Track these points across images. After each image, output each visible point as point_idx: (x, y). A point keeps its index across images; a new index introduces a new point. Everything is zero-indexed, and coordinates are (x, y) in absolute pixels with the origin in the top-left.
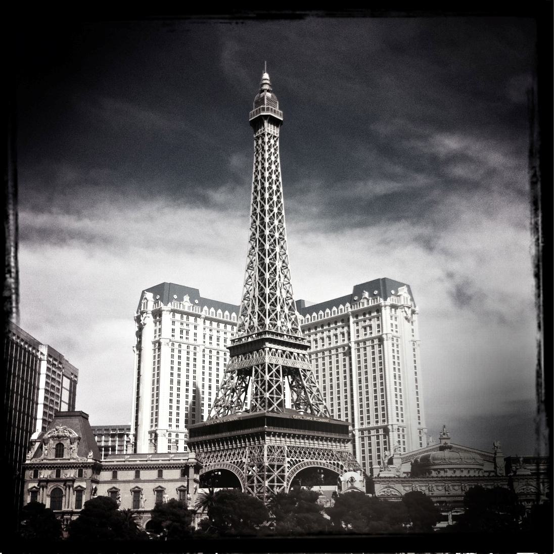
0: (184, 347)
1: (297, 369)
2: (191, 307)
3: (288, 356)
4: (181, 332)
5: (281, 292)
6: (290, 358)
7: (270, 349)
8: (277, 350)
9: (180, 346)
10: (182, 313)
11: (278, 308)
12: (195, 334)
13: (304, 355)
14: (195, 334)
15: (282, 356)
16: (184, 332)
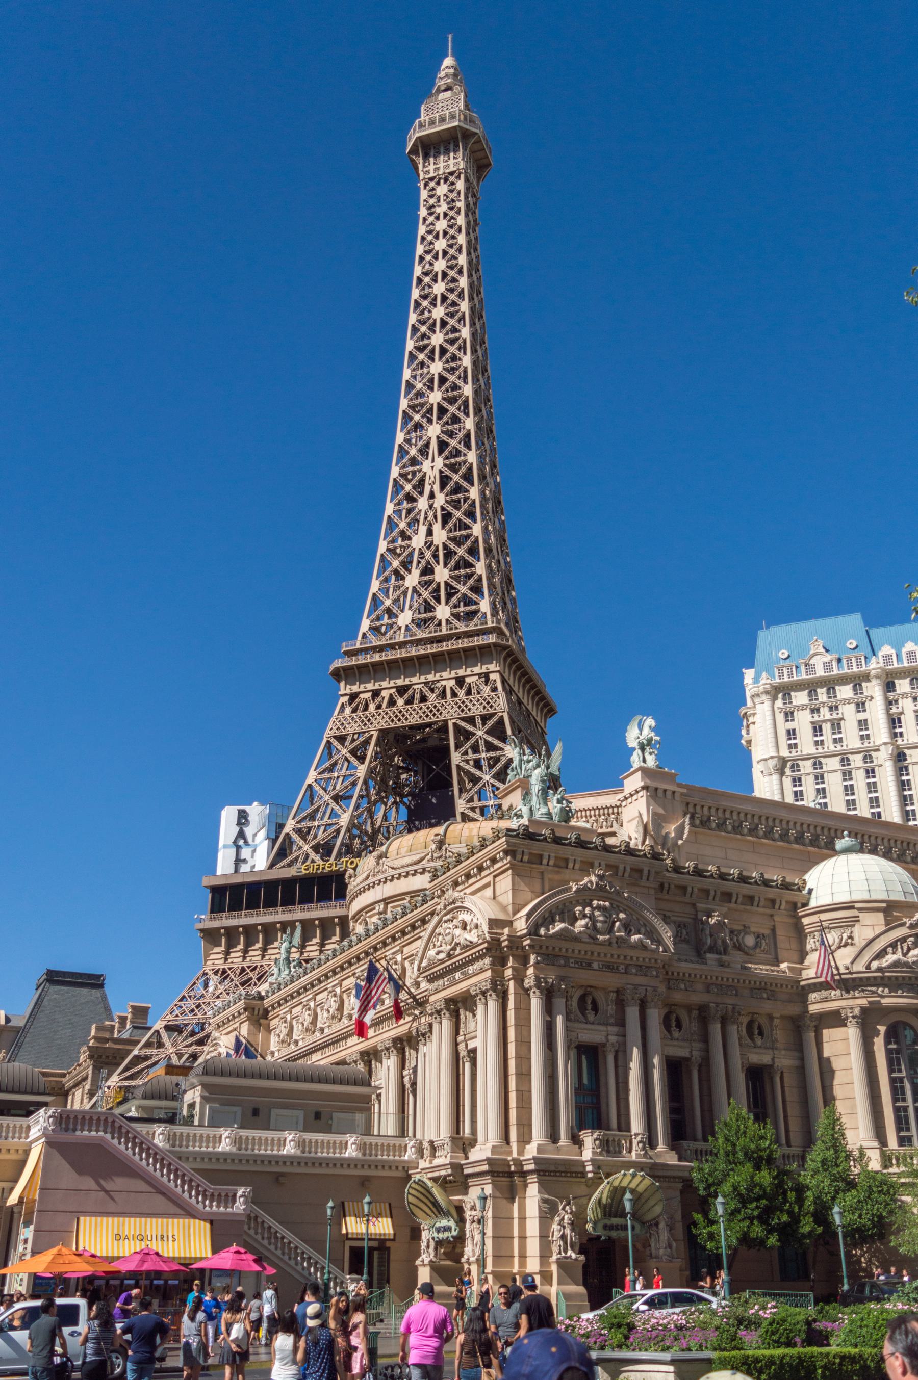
0: (832, 764)
1: (446, 721)
2: (835, 664)
3: (417, 696)
4: (817, 729)
5: (430, 533)
6: (424, 699)
7: (353, 697)
8: (376, 694)
9: (817, 764)
10: (811, 686)
11: (412, 579)
12: (863, 724)
13: (486, 676)
14: (863, 724)
15: (392, 702)
16: (827, 728)
